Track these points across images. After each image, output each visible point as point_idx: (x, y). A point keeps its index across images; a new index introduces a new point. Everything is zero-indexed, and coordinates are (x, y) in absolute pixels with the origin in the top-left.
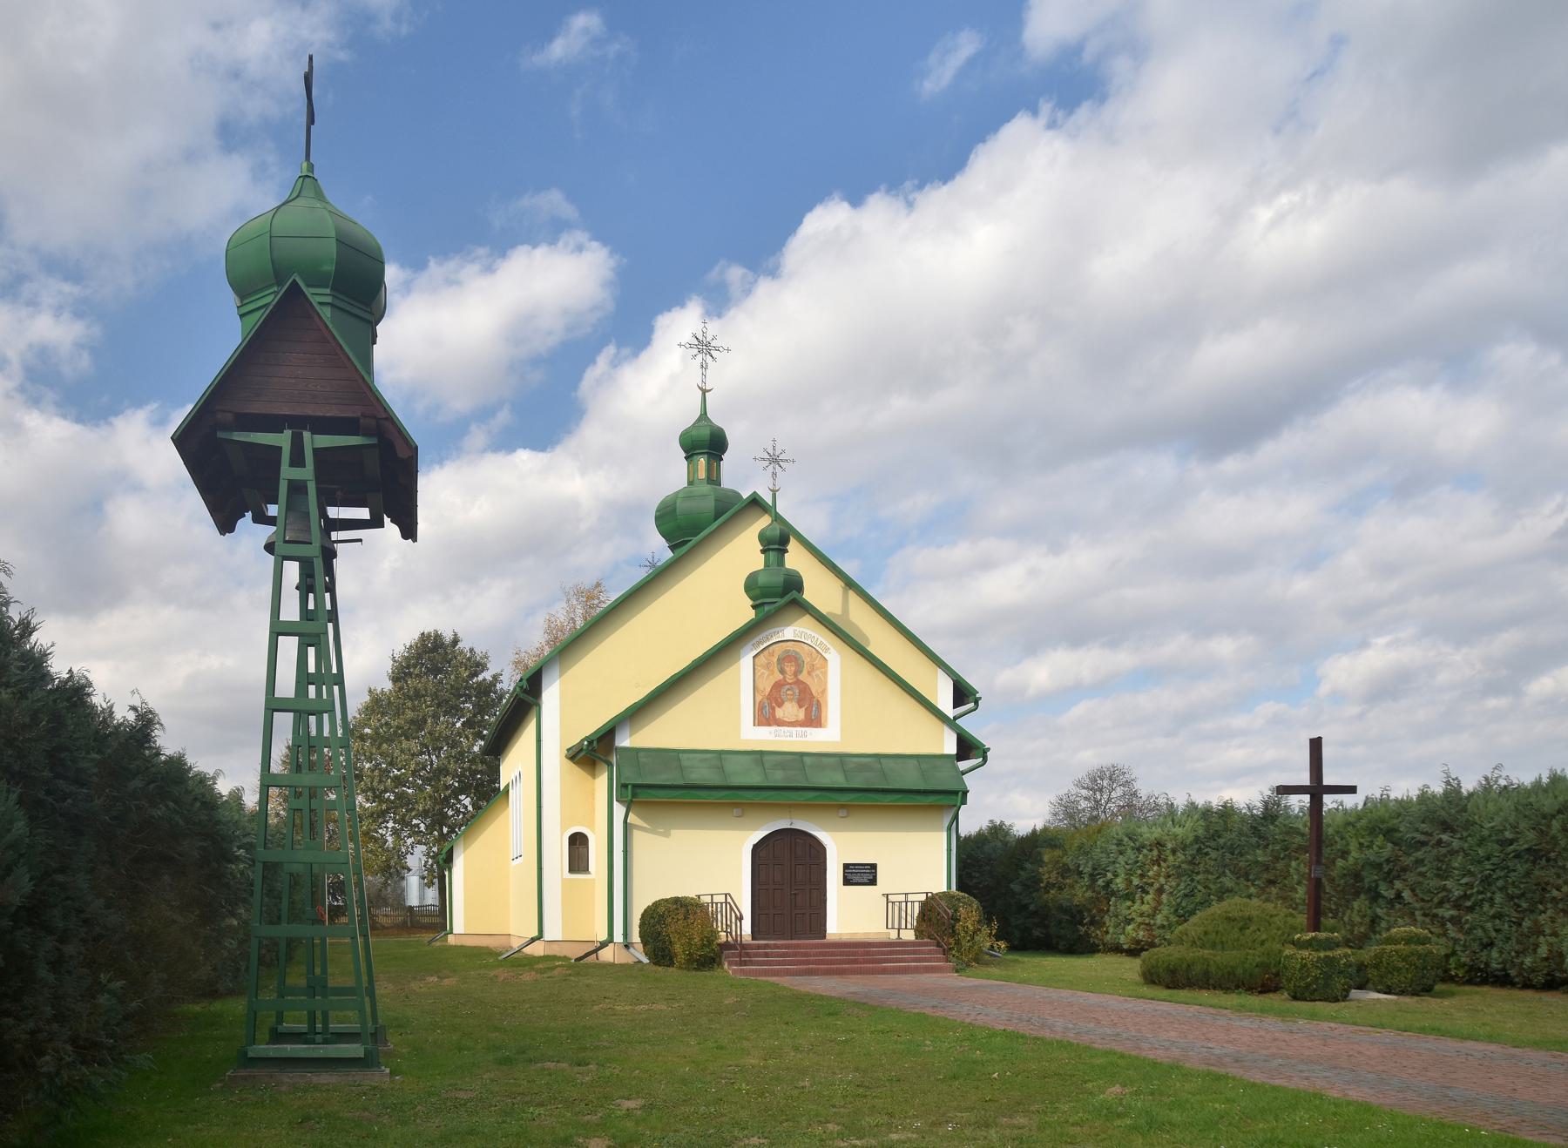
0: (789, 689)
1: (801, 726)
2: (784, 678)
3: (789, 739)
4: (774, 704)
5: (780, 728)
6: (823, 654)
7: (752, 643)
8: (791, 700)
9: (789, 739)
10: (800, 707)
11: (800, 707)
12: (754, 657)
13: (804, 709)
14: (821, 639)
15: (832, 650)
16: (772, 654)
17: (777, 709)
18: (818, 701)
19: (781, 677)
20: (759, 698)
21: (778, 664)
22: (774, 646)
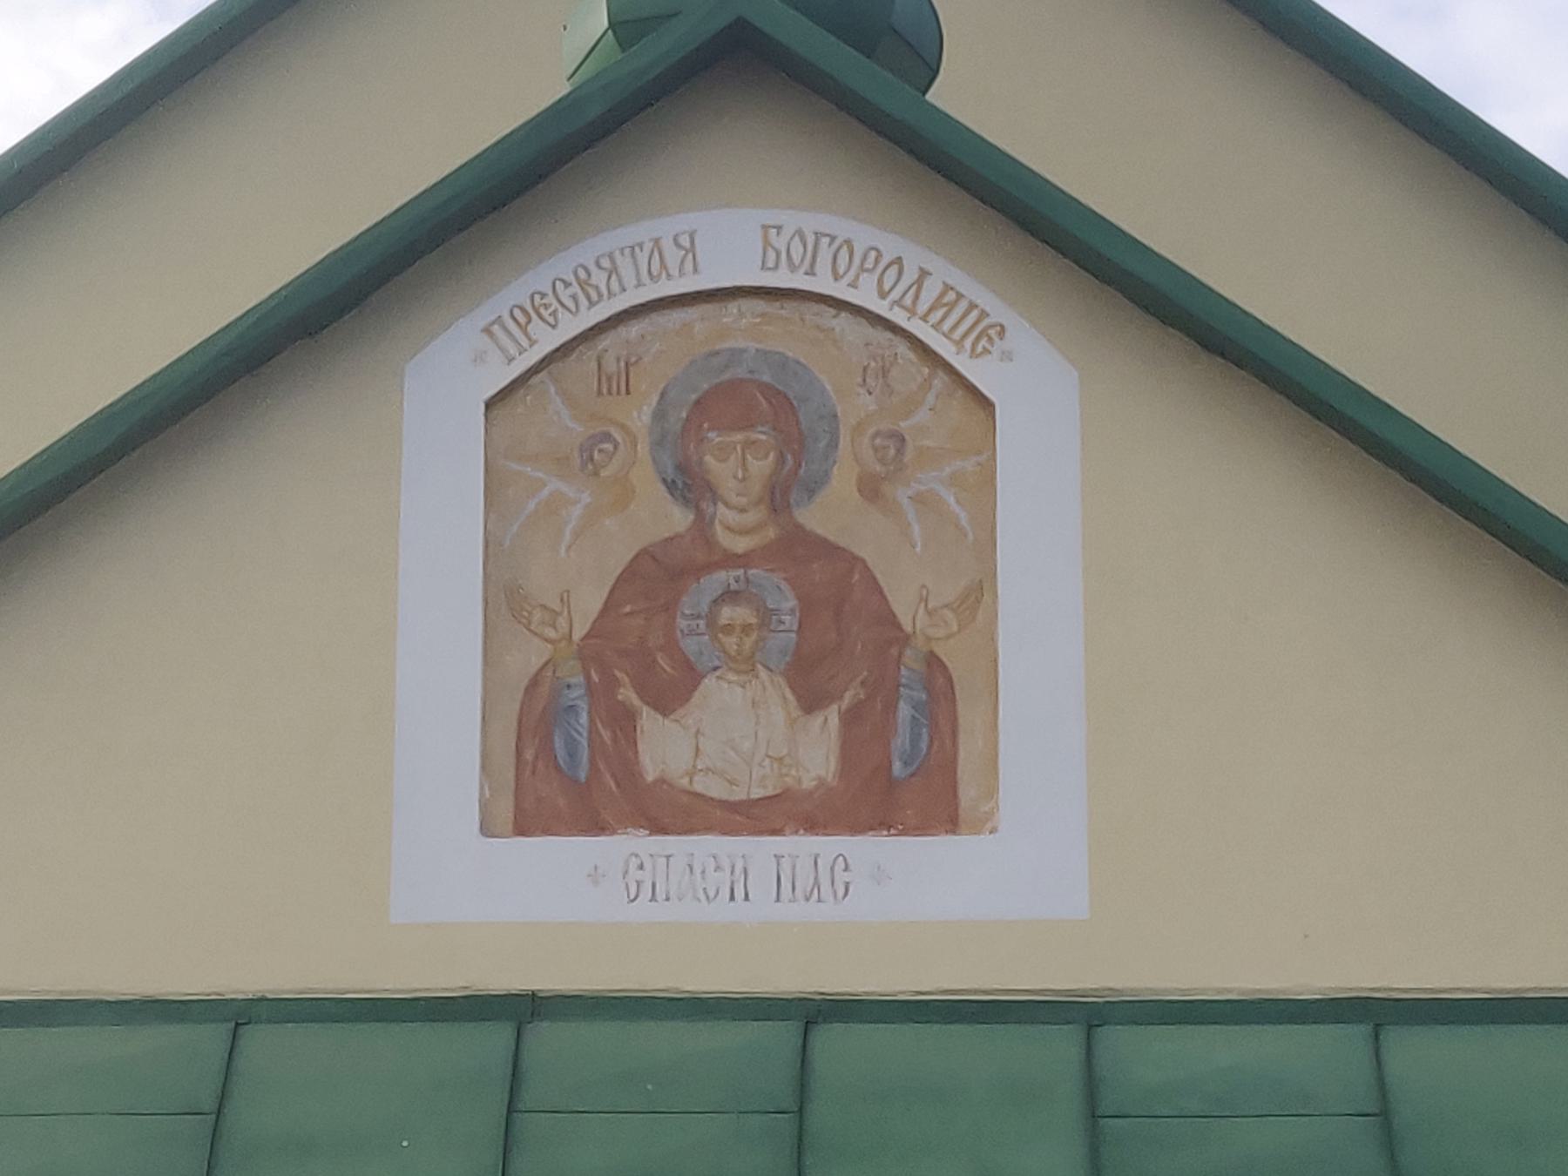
0: (730, 596)
1: (812, 825)
2: (702, 525)
4: (627, 694)
5: (671, 843)
6: (961, 363)
7: (484, 314)
8: (746, 665)
10: (810, 702)
11: (810, 702)
12: (490, 405)
13: (833, 715)
14: (944, 272)
15: (1024, 338)
16: (621, 383)
17: (648, 720)
18: (934, 662)
19: (679, 519)
20: (528, 656)
21: (658, 443)
22: (633, 330)
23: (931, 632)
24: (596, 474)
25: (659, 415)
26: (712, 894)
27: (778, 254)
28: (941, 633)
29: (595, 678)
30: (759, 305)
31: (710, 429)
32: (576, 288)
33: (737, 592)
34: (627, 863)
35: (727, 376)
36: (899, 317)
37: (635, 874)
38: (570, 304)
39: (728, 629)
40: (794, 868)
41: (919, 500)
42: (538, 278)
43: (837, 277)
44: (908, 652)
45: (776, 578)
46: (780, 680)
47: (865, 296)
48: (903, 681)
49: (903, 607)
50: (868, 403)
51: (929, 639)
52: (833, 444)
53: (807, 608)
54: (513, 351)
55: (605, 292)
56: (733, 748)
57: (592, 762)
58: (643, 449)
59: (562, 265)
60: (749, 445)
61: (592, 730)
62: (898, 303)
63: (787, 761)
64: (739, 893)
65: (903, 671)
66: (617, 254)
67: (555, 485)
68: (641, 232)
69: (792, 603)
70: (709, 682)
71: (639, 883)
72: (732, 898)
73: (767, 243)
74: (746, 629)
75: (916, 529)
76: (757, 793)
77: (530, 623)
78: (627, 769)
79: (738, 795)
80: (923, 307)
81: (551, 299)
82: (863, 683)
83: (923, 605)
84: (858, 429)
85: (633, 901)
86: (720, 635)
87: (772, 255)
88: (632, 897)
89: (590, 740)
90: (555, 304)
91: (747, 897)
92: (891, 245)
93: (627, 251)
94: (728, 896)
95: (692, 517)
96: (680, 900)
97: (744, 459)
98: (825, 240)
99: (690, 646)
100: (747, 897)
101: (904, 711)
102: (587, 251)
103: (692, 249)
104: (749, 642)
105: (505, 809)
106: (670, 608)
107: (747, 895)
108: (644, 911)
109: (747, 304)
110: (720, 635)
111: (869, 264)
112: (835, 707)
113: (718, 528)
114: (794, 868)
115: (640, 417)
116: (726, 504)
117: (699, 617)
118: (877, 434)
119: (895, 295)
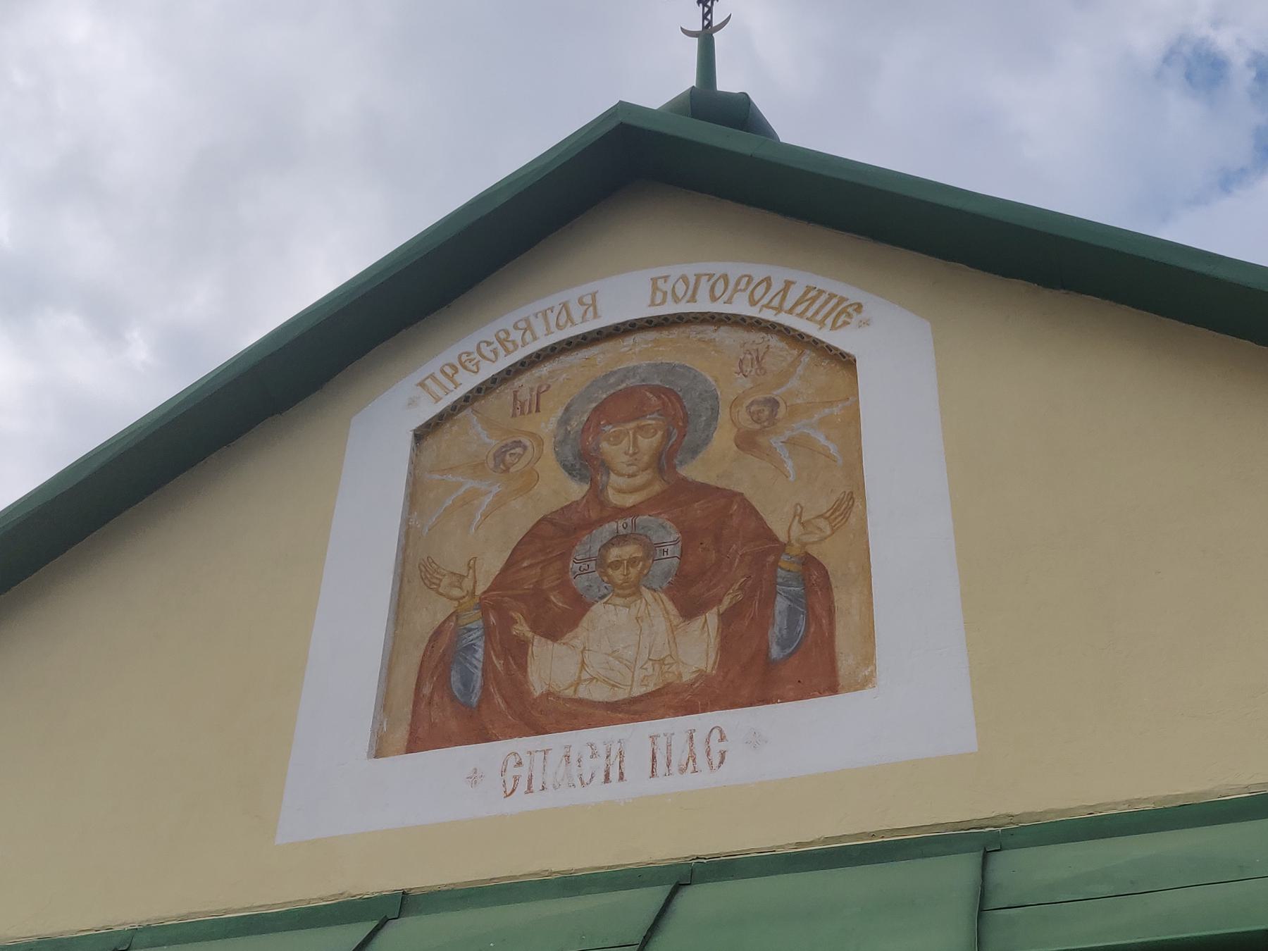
0: (618, 539)
1: (689, 708)
2: (596, 493)
3: (598, 793)
4: (522, 628)
5: (555, 741)
8: (633, 590)
9: (598, 793)
10: (690, 609)
11: (690, 609)
12: (422, 435)
13: (712, 618)
14: (803, 279)
15: (875, 306)
18: (809, 562)
19: (577, 490)
21: (560, 443)
22: (544, 370)
23: (805, 538)
24: (507, 470)
25: (564, 421)
26: (586, 779)
27: (665, 293)
28: (815, 538)
29: (492, 619)
30: (651, 335)
31: (609, 423)
32: (497, 345)
33: (625, 536)
34: (505, 762)
35: (623, 386)
36: (768, 315)
37: (512, 771)
38: (492, 356)
39: (617, 564)
40: (669, 745)
41: (791, 443)
42: (468, 344)
43: (714, 299)
44: (784, 557)
45: (663, 519)
46: (663, 596)
47: (741, 307)
48: (780, 580)
49: (779, 528)
50: (743, 383)
51: (804, 545)
52: (715, 412)
53: (689, 537)
54: (440, 393)
55: (520, 343)
56: (616, 658)
57: (485, 688)
58: (548, 448)
59: (487, 332)
60: (640, 428)
61: (487, 654)
62: (767, 306)
63: (669, 660)
64: (614, 775)
65: (780, 572)
66: (532, 319)
67: (470, 484)
68: (554, 300)
69: (675, 535)
70: (598, 608)
71: (516, 779)
72: (607, 779)
73: (655, 289)
74: (633, 562)
75: (789, 465)
76: (638, 691)
77: (439, 585)
78: (516, 689)
79: (622, 694)
80: (788, 304)
81: (476, 355)
82: (740, 588)
83: (797, 518)
84: (735, 403)
85: (507, 796)
86: (610, 571)
87: (659, 296)
88: (508, 792)
89: (484, 671)
90: (479, 358)
91: (621, 778)
92: (759, 271)
93: (540, 315)
94: (603, 779)
95: (586, 487)
96: (555, 788)
97: (635, 439)
98: (704, 279)
99: (580, 583)
100: (621, 778)
101: (781, 604)
102: (506, 321)
103: (594, 305)
104: (633, 572)
105: (401, 734)
106: (565, 556)
107: (622, 774)
108: (521, 803)
109: (639, 337)
110: (610, 571)
111: (742, 286)
112: (715, 609)
113: (610, 492)
114: (669, 745)
115: (546, 424)
116: (620, 474)
117: (590, 559)
118: (752, 404)
119: (765, 301)
